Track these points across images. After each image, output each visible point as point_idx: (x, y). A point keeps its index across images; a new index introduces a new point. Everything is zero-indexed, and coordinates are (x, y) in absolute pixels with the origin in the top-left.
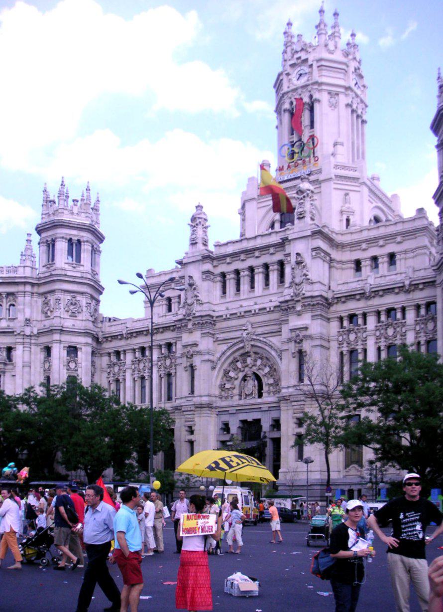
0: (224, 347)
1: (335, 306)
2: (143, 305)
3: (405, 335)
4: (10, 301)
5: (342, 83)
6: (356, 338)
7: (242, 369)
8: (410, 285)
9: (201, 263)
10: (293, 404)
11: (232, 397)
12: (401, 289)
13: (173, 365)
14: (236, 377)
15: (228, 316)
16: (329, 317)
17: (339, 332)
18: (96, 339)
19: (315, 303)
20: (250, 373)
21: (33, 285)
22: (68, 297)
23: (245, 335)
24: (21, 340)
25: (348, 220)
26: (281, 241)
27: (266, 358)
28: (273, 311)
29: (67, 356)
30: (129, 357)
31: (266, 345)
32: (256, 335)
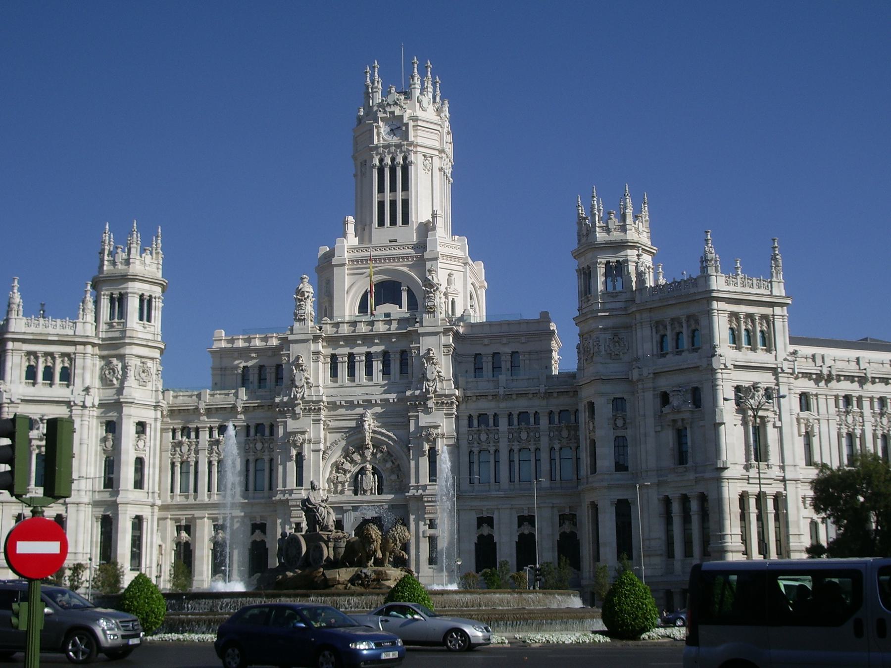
1: (465, 403)
2: (210, 371)
3: (539, 440)
5: (437, 145)
8: (545, 393)
10: (426, 504)
12: (535, 395)
13: (266, 450)
15: (343, 403)
16: (459, 414)
18: (162, 412)
20: (369, 467)
22: (138, 362)
25: (453, 303)
29: (137, 433)
30: (205, 436)
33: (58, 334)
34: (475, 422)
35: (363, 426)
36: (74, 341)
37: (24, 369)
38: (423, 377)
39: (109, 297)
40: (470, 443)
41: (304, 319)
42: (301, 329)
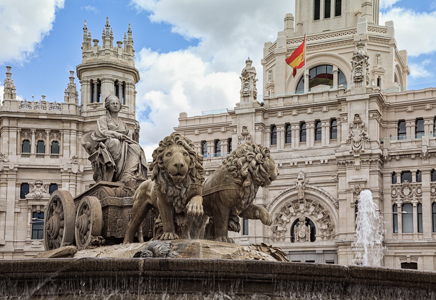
0: (277, 193)
1: (389, 163)
4: (53, 137)
6: (410, 193)
7: (294, 214)
9: (254, 115)
11: (284, 239)
14: (288, 221)
17: (392, 186)
19: (374, 160)
21: (78, 123)
23: (300, 182)
24: (67, 178)
26: (337, 101)
27: (320, 205)
28: (326, 163)
31: (320, 194)
32: (310, 184)
33: (47, 114)
34: (399, 179)
35: (298, 183)
36: (61, 120)
37: (20, 143)
38: (350, 139)
39: (89, 84)
40: (394, 197)
41: (248, 96)
42: (247, 105)
